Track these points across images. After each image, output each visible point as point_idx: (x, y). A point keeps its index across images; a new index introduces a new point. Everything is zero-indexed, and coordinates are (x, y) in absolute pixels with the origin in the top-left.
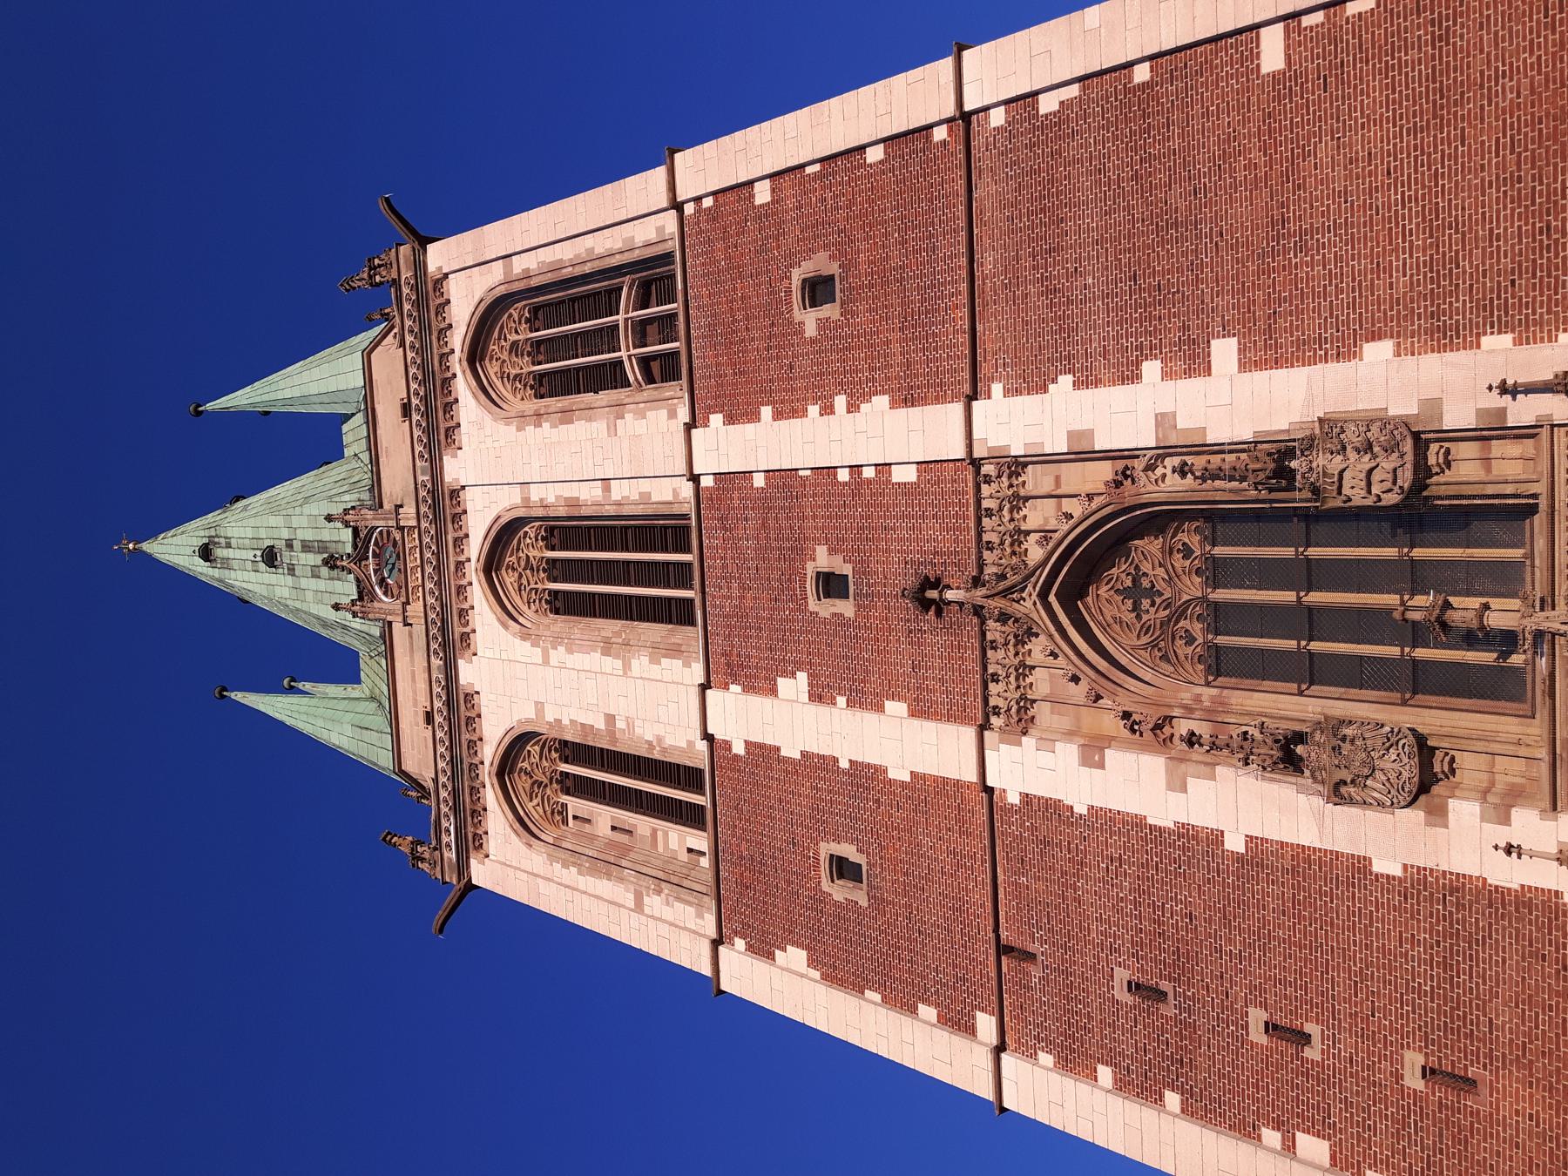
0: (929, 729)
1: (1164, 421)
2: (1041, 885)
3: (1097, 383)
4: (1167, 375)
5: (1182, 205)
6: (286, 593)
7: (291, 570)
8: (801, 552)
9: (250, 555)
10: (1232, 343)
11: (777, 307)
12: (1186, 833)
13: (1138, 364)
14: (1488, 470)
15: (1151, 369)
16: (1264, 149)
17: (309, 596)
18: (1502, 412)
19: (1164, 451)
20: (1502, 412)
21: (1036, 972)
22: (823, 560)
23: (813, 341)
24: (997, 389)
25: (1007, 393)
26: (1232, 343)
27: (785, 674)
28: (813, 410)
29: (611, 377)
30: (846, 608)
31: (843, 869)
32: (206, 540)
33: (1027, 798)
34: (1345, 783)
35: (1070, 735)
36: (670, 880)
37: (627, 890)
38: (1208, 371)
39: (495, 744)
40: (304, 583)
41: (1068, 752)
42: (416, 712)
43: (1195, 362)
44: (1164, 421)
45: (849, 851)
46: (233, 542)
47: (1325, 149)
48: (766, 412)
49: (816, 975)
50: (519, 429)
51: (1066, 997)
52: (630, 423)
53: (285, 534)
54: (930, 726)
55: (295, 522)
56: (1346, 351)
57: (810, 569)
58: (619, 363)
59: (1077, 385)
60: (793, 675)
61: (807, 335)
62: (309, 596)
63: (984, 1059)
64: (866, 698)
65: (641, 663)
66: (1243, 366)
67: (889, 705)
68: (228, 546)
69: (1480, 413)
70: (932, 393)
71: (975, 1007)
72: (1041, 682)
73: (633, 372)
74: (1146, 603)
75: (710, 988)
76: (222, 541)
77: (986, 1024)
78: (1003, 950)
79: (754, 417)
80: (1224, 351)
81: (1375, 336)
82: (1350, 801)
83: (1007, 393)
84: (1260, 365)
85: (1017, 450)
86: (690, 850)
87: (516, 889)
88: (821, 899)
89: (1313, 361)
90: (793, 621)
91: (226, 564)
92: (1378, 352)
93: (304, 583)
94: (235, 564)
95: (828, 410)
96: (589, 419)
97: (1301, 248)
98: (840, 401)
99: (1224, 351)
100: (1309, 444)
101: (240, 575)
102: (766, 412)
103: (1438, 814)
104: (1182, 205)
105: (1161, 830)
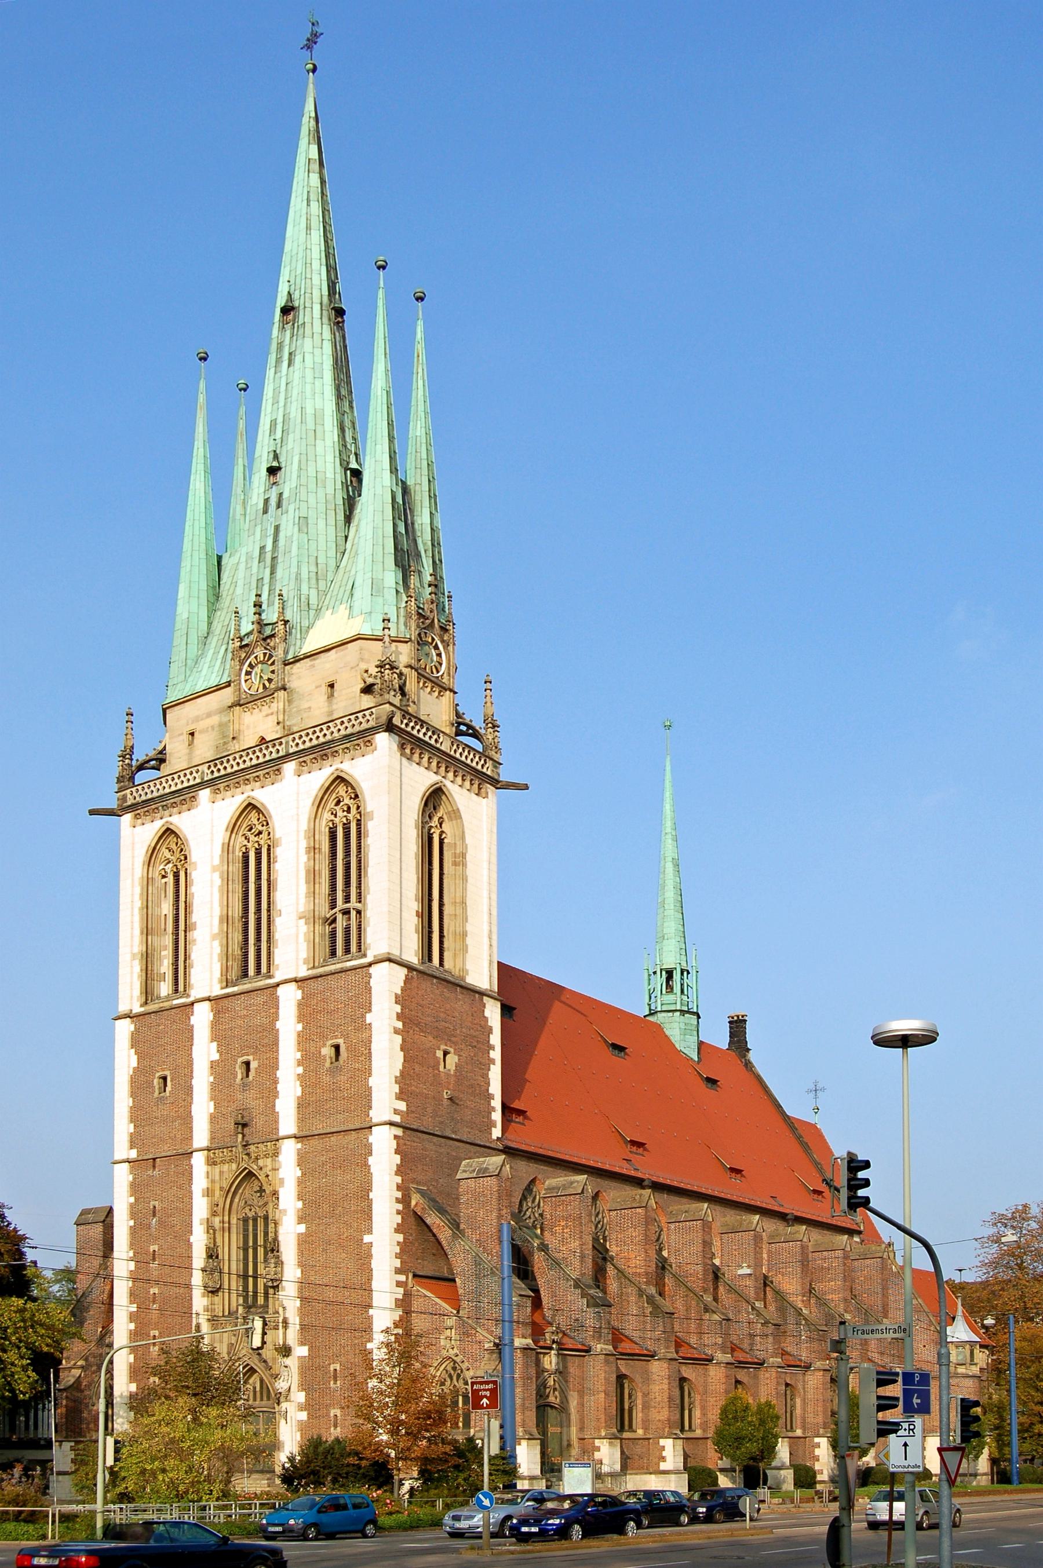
22: (254, 1065)
24: (299, 1146)
28: (299, 1055)
32: (296, 304)
35: (213, 1181)
43: (301, 1220)
49: (131, 1073)
63: (125, 1157)
67: (212, 1103)
72: (226, 1167)
77: (133, 1154)
78: (154, 1159)
80: (302, 1228)
98: (300, 1070)
99: (302, 1228)
100: (278, 1257)
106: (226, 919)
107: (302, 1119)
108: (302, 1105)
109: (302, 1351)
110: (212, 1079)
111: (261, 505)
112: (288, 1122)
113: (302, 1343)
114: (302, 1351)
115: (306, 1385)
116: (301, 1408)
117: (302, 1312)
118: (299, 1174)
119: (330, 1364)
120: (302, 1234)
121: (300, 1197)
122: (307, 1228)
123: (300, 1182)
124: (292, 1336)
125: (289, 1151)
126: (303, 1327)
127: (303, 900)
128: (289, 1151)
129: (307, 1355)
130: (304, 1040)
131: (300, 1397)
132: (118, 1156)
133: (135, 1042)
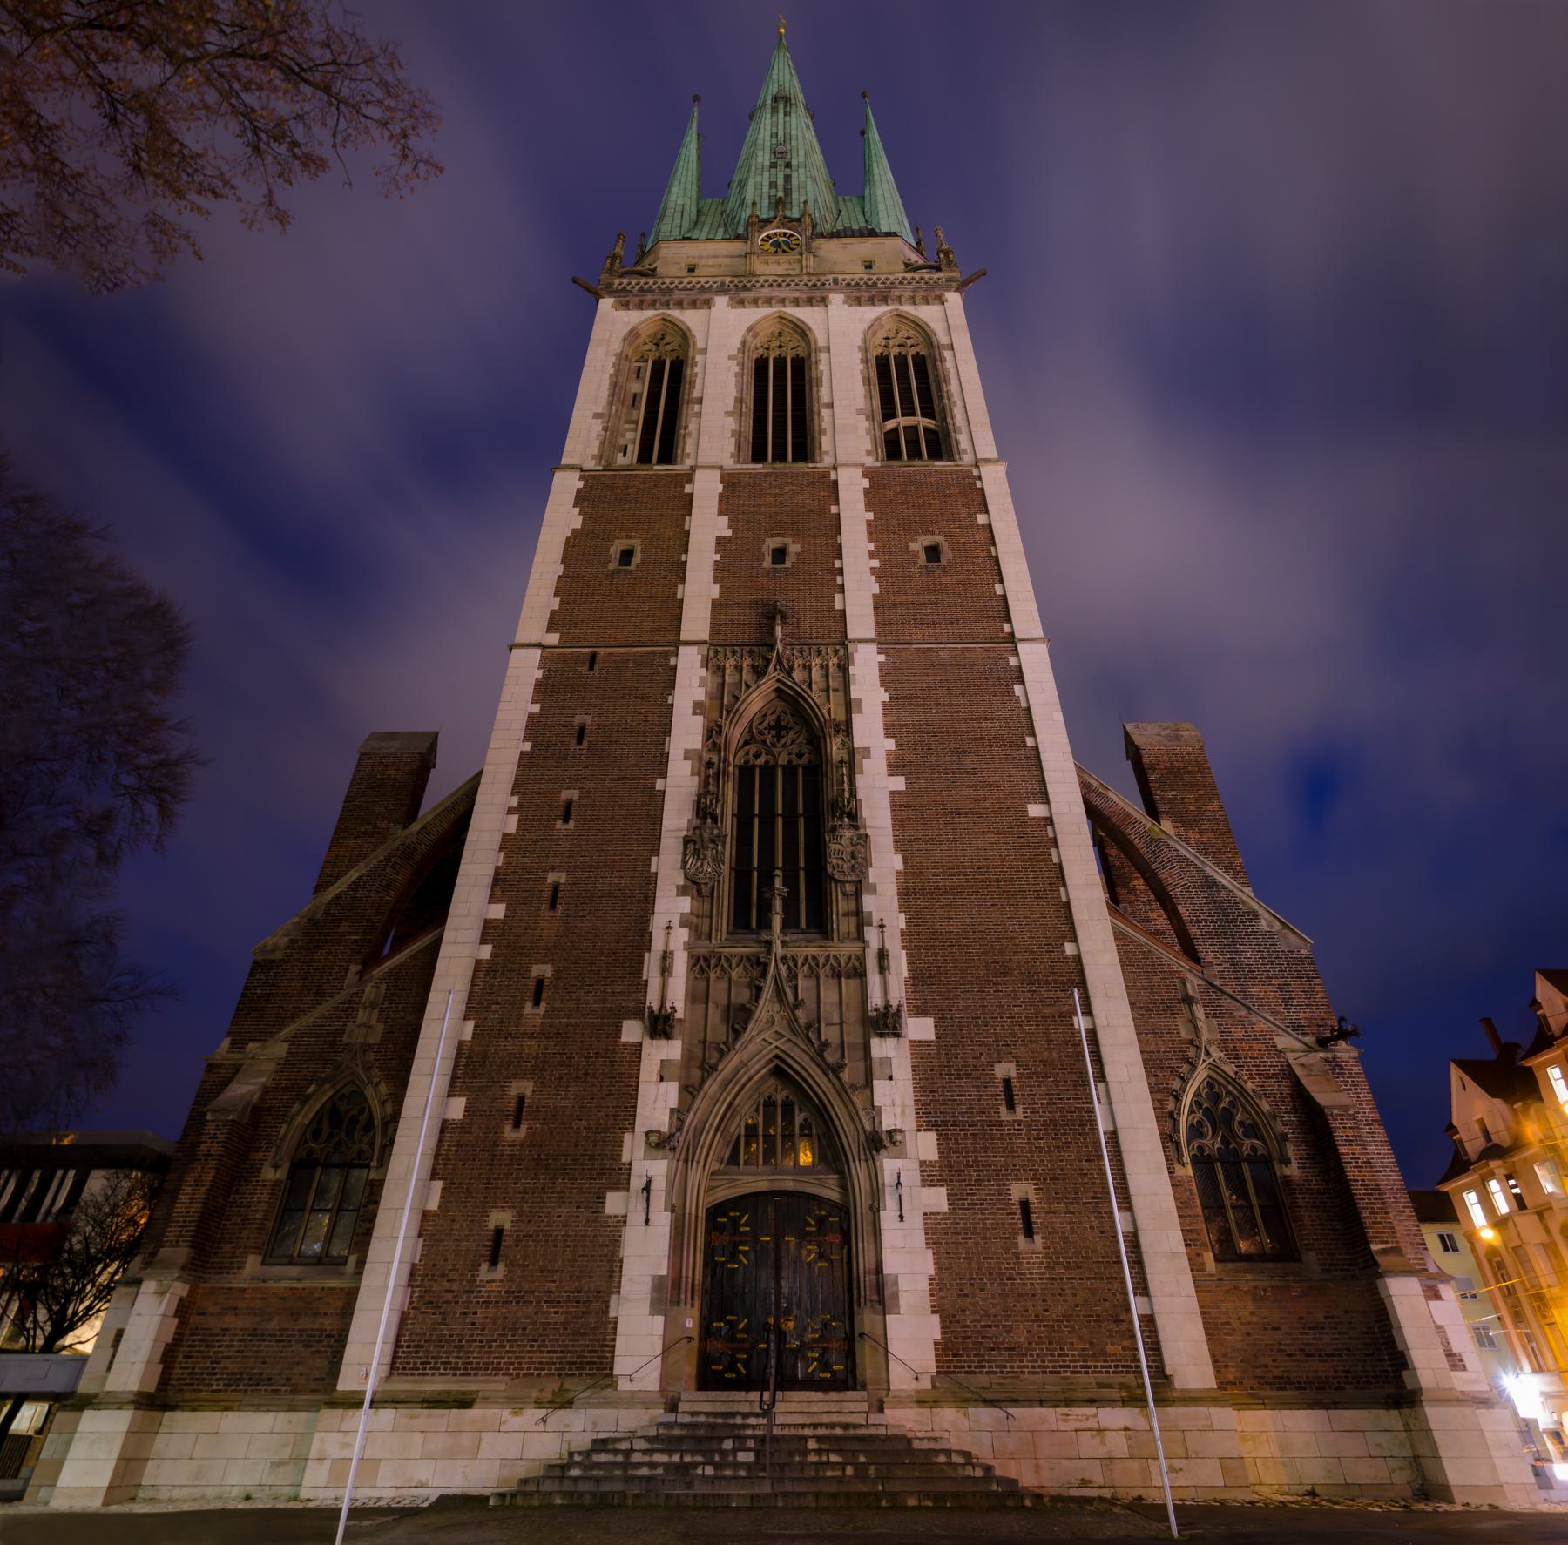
0: (706, 613)
1: (866, 752)
2: (629, 674)
3: (885, 715)
4: (888, 753)
5: (968, 762)
6: (760, 159)
7: (773, 165)
8: (797, 535)
9: (781, 134)
10: (903, 788)
11: (926, 527)
12: (664, 758)
13: (894, 737)
14: (844, 915)
15: (891, 744)
16: (992, 805)
17: (759, 179)
18: (870, 924)
19: (851, 752)
20: (870, 924)
21: (584, 669)
22: (794, 549)
23: (907, 547)
25: (880, 663)
26: (903, 788)
27: (730, 521)
29: (888, 413)
30: (767, 563)
31: (627, 555)
33: (674, 668)
34: (695, 844)
36: (610, 442)
37: (604, 408)
38: (890, 775)
39: (681, 318)
40: (766, 175)
41: (700, 695)
42: (694, 257)
43: (894, 768)
44: (866, 752)
45: (637, 559)
46: (788, 118)
47: (990, 836)
48: (870, 516)
50: (859, 347)
51: (573, 687)
52: (864, 424)
53: (794, 162)
54: (707, 614)
55: (802, 171)
56: (900, 846)
57: (788, 540)
58: (894, 416)
59: (884, 703)
60: (730, 527)
61: (910, 544)
62: (759, 179)
63: (535, 639)
64: (722, 573)
65: (731, 423)
66: (892, 793)
68: (786, 114)
69: (870, 913)
70: (880, 619)
71: (561, 632)
73: (890, 424)
74: (773, 732)
75: (556, 465)
76: (788, 109)
77: (554, 639)
79: (868, 508)
80: (899, 783)
81: (905, 860)
82: (685, 848)
83: (880, 663)
84: (892, 801)
85: (852, 670)
86: (626, 447)
87: (598, 332)
88: (610, 539)
89: (894, 829)
90: (759, 528)
91: (774, 111)
92: (897, 862)
93: (766, 175)
94: (774, 119)
95: (872, 555)
96: (865, 397)
97: (947, 824)
98: (876, 563)
99: (899, 783)
101: (768, 122)
102: (870, 516)
103: (682, 891)
104: (968, 762)
105: (664, 744)
106: (739, 401)
107: (881, 623)
108: (879, 604)
109: (920, 1028)
110: (717, 557)
111: (767, 163)
112: (861, 622)
113: (920, 1012)
114: (920, 1028)
115: (928, 1117)
116: (930, 1176)
117: (910, 937)
118: (886, 697)
119: (992, 1064)
120: (899, 792)
121: (889, 733)
122: (908, 784)
123: (887, 709)
124: (898, 992)
125: (866, 664)
126: (917, 979)
127: (862, 399)
128: (866, 664)
129: (932, 1037)
130: (873, 530)
131: (926, 1146)
132: (520, 637)
133: (580, 499)
